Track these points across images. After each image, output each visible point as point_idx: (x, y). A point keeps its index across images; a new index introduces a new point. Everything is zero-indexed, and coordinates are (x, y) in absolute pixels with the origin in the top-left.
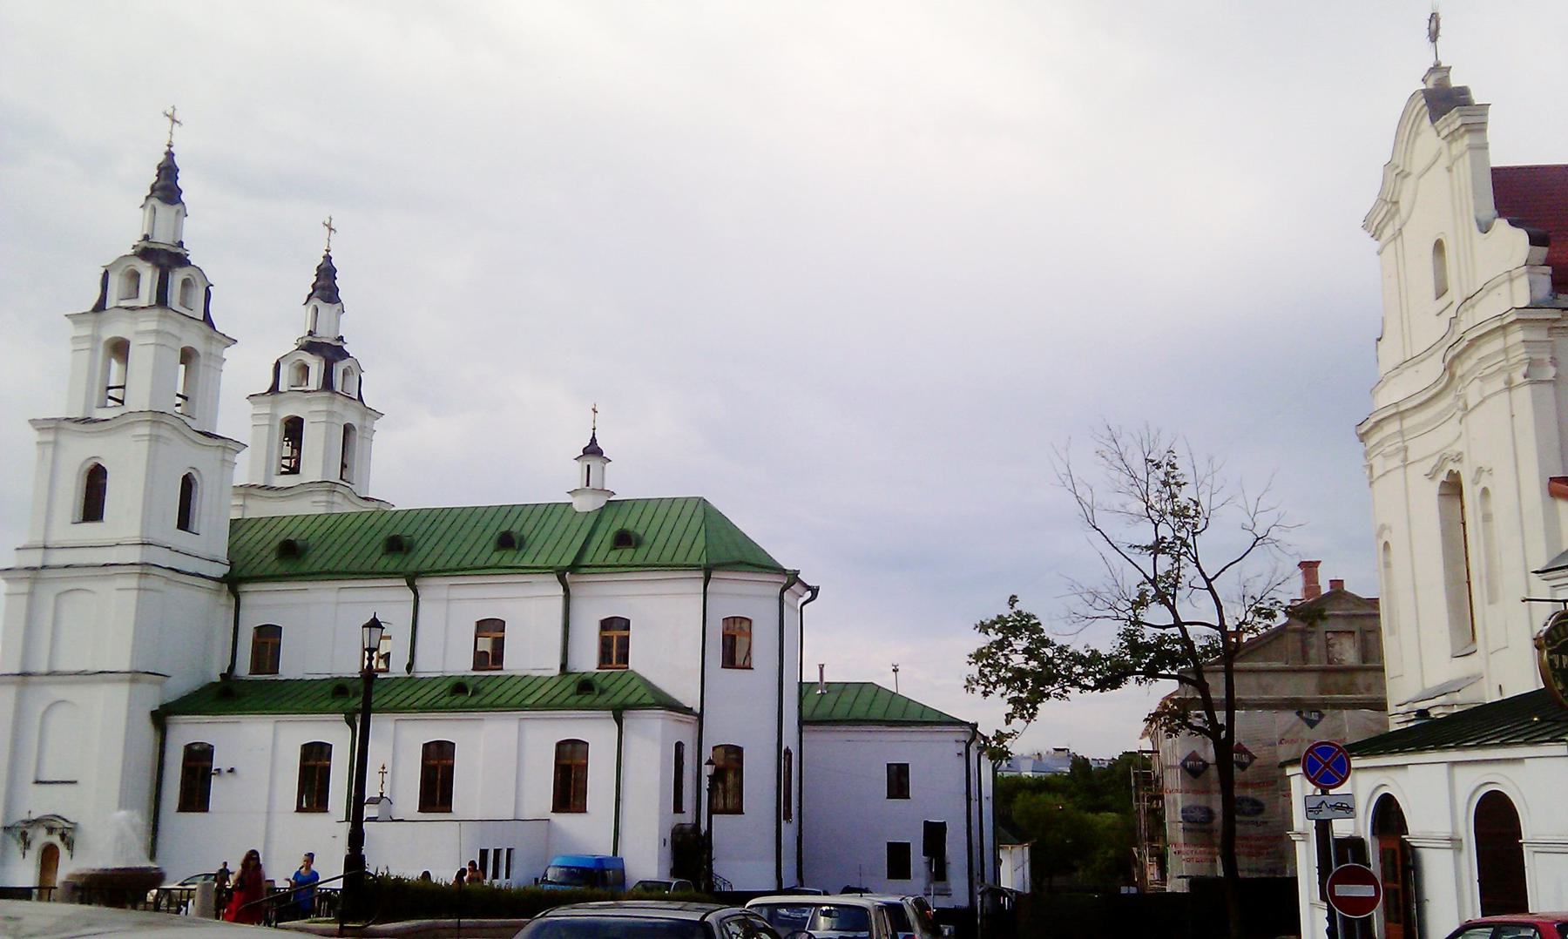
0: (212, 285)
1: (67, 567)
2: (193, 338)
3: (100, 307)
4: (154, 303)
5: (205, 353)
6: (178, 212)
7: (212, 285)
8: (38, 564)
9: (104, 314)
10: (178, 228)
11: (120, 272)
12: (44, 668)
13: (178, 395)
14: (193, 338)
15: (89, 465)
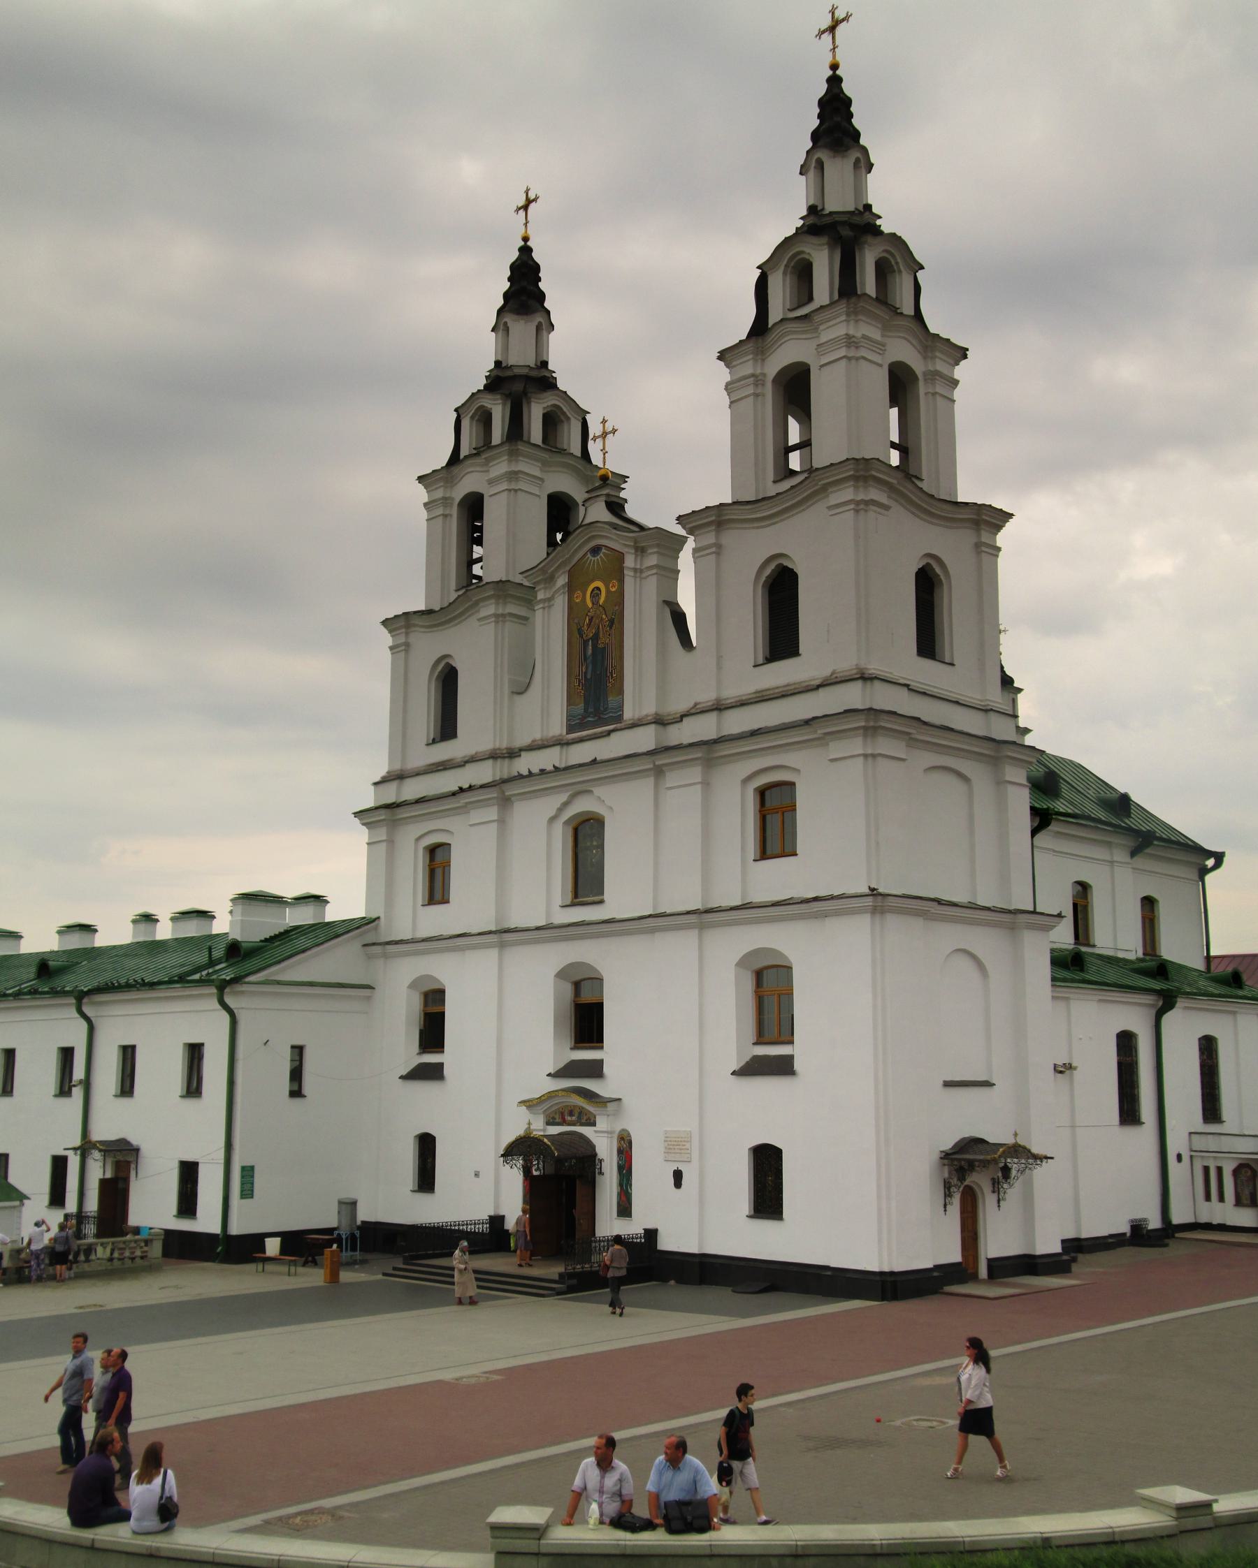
0: (922, 268)
1: (754, 733)
2: (904, 351)
3: (760, 327)
4: (836, 296)
5: (925, 374)
6: (857, 161)
7: (922, 268)
8: (713, 735)
9: (771, 337)
10: (860, 188)
11: (782, 268)
12: (738, 903)
13: (893, 445)
14: (904, 351)
15: (772, 566)
